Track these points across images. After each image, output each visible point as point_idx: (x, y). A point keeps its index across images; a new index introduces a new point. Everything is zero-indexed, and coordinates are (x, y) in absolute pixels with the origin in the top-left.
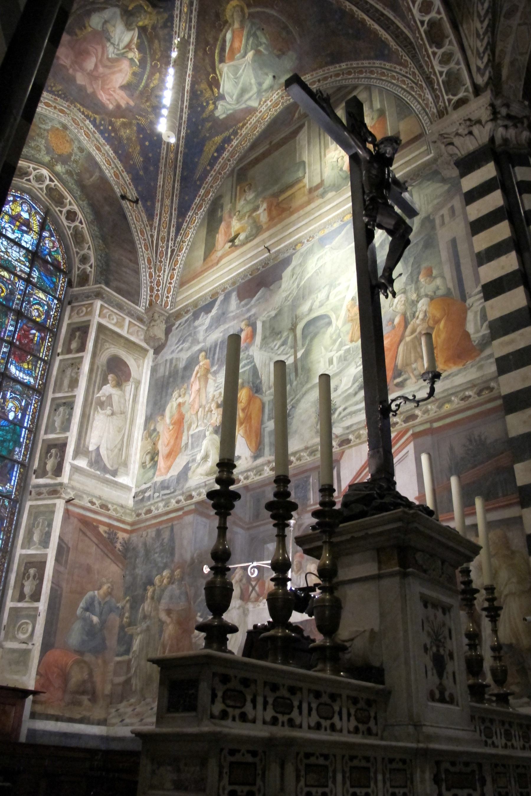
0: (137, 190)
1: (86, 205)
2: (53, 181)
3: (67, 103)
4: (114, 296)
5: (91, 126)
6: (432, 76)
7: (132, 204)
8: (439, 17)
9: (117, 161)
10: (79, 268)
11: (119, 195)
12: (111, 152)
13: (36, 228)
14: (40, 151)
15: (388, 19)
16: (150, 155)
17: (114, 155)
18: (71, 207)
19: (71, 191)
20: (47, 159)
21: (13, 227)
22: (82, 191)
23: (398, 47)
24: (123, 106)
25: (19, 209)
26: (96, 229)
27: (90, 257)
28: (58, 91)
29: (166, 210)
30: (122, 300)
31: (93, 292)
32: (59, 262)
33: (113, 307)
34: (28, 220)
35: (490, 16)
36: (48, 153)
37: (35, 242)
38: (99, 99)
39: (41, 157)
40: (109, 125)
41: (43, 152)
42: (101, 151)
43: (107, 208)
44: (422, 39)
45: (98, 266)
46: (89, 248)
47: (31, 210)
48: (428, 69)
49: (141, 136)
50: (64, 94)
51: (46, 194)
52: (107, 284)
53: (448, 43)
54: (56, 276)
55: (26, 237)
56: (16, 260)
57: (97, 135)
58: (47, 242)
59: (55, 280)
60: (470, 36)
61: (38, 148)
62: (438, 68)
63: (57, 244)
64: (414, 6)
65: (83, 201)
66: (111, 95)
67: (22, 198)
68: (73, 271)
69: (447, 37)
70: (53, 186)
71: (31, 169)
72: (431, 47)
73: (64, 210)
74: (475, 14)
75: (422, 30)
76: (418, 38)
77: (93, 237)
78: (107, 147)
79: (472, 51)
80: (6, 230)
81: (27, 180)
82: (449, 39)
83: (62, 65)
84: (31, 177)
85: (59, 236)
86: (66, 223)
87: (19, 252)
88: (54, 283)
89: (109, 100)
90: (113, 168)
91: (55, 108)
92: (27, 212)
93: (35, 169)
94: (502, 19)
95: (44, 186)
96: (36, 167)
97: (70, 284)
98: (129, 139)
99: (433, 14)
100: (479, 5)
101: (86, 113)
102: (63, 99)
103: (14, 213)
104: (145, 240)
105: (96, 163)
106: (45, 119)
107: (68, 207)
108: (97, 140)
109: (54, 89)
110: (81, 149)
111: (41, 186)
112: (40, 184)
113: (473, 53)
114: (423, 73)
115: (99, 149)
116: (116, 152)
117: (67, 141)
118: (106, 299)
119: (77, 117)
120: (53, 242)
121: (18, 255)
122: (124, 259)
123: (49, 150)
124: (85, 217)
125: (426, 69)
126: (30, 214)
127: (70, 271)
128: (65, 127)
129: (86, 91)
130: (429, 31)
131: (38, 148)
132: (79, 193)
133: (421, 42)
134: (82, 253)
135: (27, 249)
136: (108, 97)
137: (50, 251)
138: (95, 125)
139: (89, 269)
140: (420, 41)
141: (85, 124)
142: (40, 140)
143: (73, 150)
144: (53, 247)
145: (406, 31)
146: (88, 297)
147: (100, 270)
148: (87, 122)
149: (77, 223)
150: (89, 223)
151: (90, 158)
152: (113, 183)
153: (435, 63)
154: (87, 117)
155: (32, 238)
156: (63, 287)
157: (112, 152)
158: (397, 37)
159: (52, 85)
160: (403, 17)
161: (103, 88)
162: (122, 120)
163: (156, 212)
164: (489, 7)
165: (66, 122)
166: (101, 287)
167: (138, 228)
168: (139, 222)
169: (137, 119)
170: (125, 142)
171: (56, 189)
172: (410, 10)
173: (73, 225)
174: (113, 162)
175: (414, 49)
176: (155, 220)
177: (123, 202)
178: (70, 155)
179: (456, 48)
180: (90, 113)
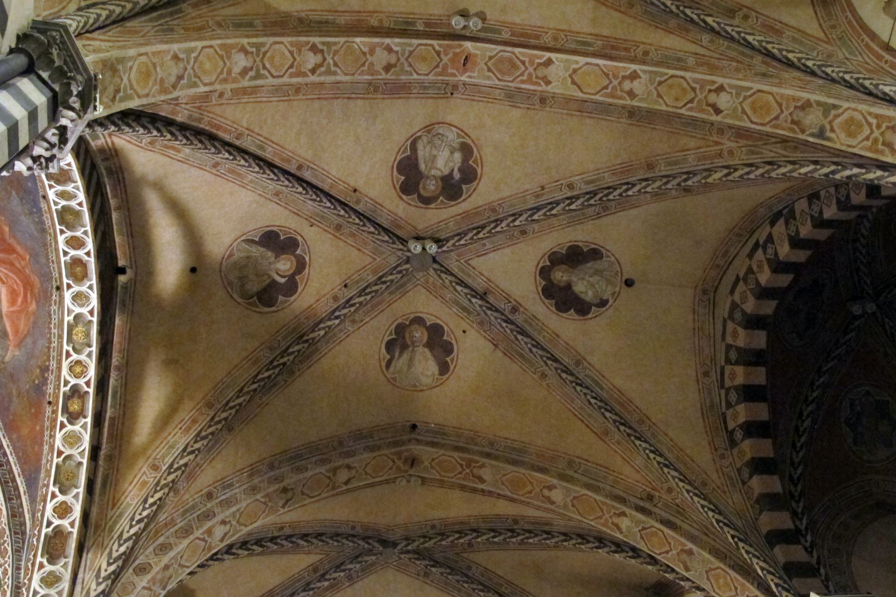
6: (24, 589)
8: (70, 529)
15: (16, 488)
23: (7, 528)
35: (120, 563)
44: (38, 540)
48: (24, 578)
53: (62, 564)
60: (90, 570)
62: (35, 584)
64: (51, 501)
69: (65, 557)
72: (42, 556)
74: (108, 550)
75: (44, 531)
76: (35, 535)
79: (82, 588)
82: (67, 560)
94: (131, 570)
99: (65, 523)
100: (116, 544)
113: (81, 593)
114: (16, 577)
125: (22, 575)
130: (51, 538)
133: (35, 543)
140: (35, 540)
145: (27, 516)
153: (36, 577)
158: (14, 516)
160: (33, 500)
164: (124, 553)
172: (45, 501)
175: (24, 543)
179: (67, 576)
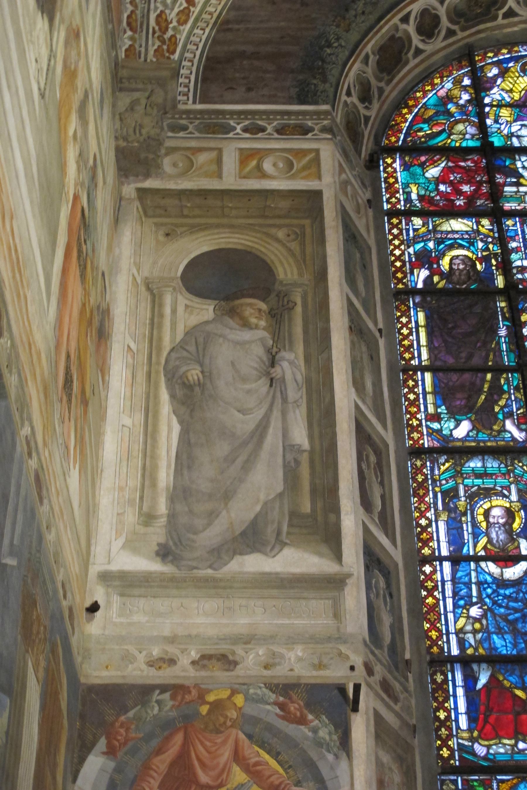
80: (518, 137)
81: (506, 16)
103: (517, 96)
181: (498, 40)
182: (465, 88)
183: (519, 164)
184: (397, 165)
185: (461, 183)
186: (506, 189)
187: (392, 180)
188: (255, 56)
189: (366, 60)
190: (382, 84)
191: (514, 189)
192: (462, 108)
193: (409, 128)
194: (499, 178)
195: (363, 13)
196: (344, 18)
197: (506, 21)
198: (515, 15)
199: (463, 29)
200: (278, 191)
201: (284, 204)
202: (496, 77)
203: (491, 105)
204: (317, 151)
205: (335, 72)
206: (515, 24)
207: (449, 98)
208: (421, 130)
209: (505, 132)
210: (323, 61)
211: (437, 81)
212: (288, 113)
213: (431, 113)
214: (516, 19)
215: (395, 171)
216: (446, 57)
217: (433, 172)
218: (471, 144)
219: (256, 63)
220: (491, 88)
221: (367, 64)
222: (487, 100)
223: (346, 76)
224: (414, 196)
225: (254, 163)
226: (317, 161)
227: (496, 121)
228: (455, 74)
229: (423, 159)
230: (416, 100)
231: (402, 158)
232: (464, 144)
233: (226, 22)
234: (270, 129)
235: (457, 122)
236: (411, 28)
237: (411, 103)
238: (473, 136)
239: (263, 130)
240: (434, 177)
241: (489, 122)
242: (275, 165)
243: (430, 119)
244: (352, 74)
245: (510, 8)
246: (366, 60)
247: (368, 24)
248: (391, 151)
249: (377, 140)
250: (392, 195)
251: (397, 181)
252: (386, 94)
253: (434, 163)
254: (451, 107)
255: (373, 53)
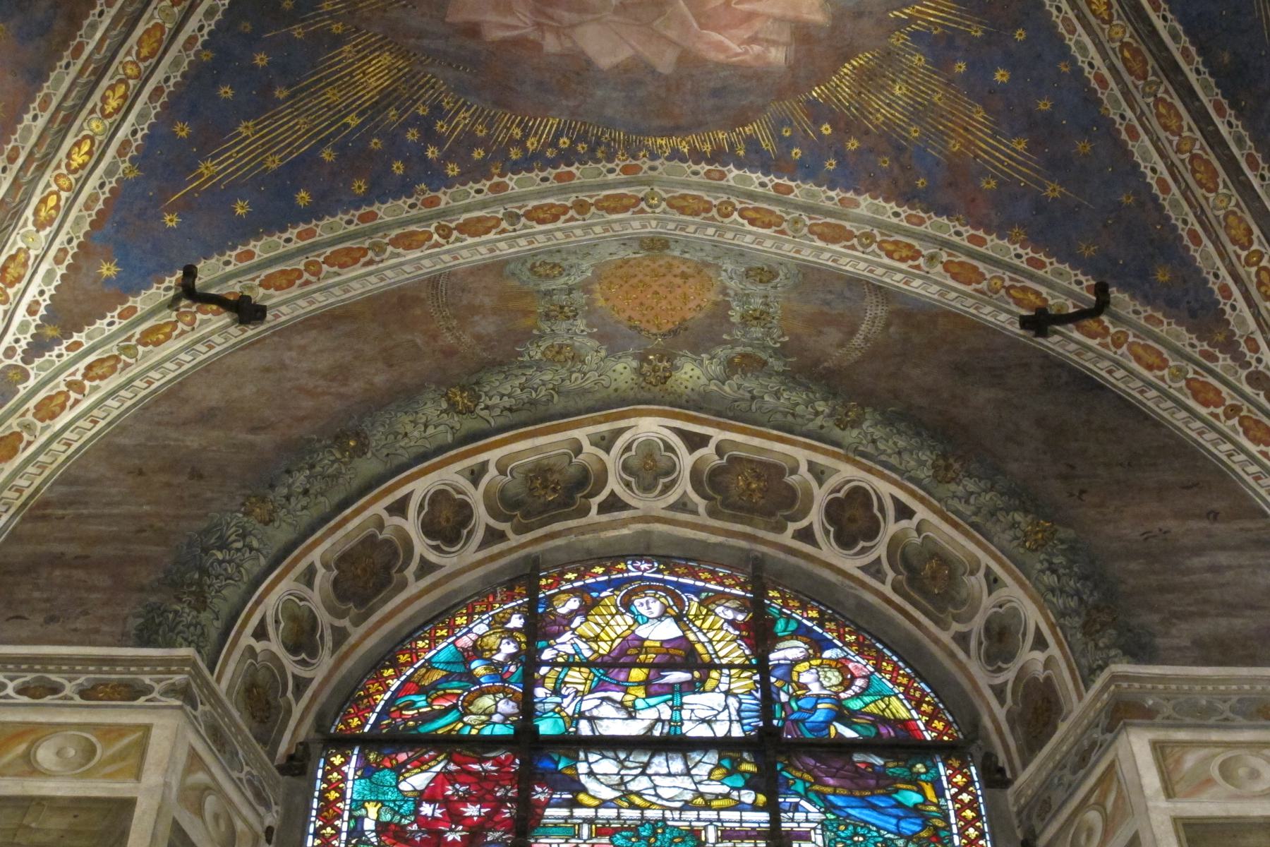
0: (1077, 262)
1: (878, 433)
2: (703, 441)
3: (618, 163)
4: (1204, 680)
5: (757, 177)
7: (1090, 324)
9: (935, 225)
10: (999, 692)
11: (1016, 329)
12: (889, 210)
13: (731, 650)
14: (577, 358)
16: (1044, 106)
17: (905, 211)
18: (832, 482)
19: (788, 427)
20: (623, 371)
21: (618, 696)
22: (831, 393)
24: (818, 17)
25: (621, 624)
26: (971, 486)
27: (1015, 613)
28: (554, 143)
29: (1239, 233)
30: (1253, 680)
31: (1094, 725)
32: (906, 724)
33: (1225, 725)
34: (684, 637)
36: (614, 352)
37: (749, 702)
38: (720, 65)
39: (593, 376)
40: (817, 122)
41: (593, 353)
42: (851, 235)
43: (983, 396)
45: (1062, 614)
46: (993, 582)
47: (679, 602)
49: (961, 67)
50: (583, 137)
51: (712, 513)
52: (1140, 651)
54: (914, 782)
55: (701, 704)
56: (687, 806)
57: (801, 191)
58: (806, 678)
59: (913, 798)
61: (567, 352)
63: (860, 665)
65: (856, 424)
66: (750, 16)
67: (616, 585)
68: (987, 721)
70: (716, 461)
71: (587, 447)
73: (815, 517)
77: (978, 529)
78: (865, 204)
80: (592, 719)
81: (603, 508)
83: (504, 41)
84: (614, 485)
85: (858, 630)
86: (850, 563)
87: (688, 773)
88: (916, 811)
89: (753, 40)
90: (932, 259)
91: (582, 207)
92: (664, 614)
93: (605, 443)
95: (685, 485)
96: (604, 428)
97: (995, 778)
98: (917, 113)
101: (707, 148)
102: (591, 156)
103: (604, 648)
104: (1233, 411)
105: (854, 282)
106: (557, 259)
107: (821, 496)
108: (810, 209)
109: (532, 144)
110: (764, 274)
111: (673, 497)
112: (667, 488)
115: (835, 235)
116: (907, 197)
117: (684, 276)
118: (1167, 709)
119: (687, 185)
120: (840, 665)
121: (686, 782)
122: (1171, 524)
123: (611, 341)
124: (905, 476)
126: (678, 619)
127: (973, 728)
128: (657, 245)
129: (653, 71)
131: (567, 352)
132: (821, 406)
134: (977, 624)
135: (723, 745)
136: (745, 33)
137: (838, 702)
138: (767, 166)
139: (1039, 656)
141: (729, 190)
142: (561, 327)
143: (724, 291)
144: (847, 683)
146: (1083, 758)
147: (1077, 621)
148: (733, 173)
149: (891, 528)
150: (928, 493)
151: (810, 276)
152: (967, 307)
154: (719, 156)
155: (728, 693)
156: (972, 805)
157: (891, 207)
159: (517, 133)
161: (707, 20)
162: (847, 69)
163: (1214, 285)
165: (653, 227)
166: (1114, 678)
167: (1177, 388)
168: (1163, 365)
169: (901, 24)
170: (915, 132)
171: (735, 463)
173: (881, 551)
174: (924, 238)
176: (1229, 314)
177: (1052, 343)
178: (721, 310)
180: (721, 135)
181: (589, 551)
182: (510, 634)
183: (582, 768)
184: (350, 770)
185: (464, 800)
186: (549, 812)
187: (333, 795)
188: (82, 562)
189: (308, 577)
190: (345, 623)
191: (564, 812)
192: (497, 669)
193: (389, 703)
194: (540, 794)
195: (306, 492)
196: (263, 499)
197: (605, 518)
198: (625, 506)
199: (519, 530)
200: (52, 799)
201: (56, 823)
202: (574, 614)
203: (552, 664)
204: (147, 728)
205: (231, 593)
206: (624, 523)
207: (477, 651)
208: (410, 705)
209: (570, 711)
210: (204, 571)
211: (460, 621)
212: (112, 661)
213: (436, 676)
214: (625, 514)
215: (344, 778)
216: (486, 579)
217: (418, 781)
218: (500, 730)
219: (79, 574)
220: (560, 634)
221: (310, 584)
222: (547, 655)
223: (258, 603)
224: (369, 825)
225: (21, 748)
226: (141, 747)
227: (556, 692)
228: (497, 609)
229: (403, 757)
230: (415, 654)
231: (363, 756)
232: (487, 731)
233: (45, 504)
234: (69, 689)
235: (482, 693)
236: (411, 525)
237: (403, 659)
238: (506, 717)
239: (55, 689)
240: (415, 790)
241: (540, 692)
242: (59, 753)
243: (434, 686)
244: (273, 600)
245: (613, 493)
246: (308, 577)
247: (314, 513)
248: (344, 743)
249: (321, 723)
250: (328, 822)
251: (342, 798)
252: (352, 640)
253: (421, 765)
254: (478, 667)
255: (326, 566)
